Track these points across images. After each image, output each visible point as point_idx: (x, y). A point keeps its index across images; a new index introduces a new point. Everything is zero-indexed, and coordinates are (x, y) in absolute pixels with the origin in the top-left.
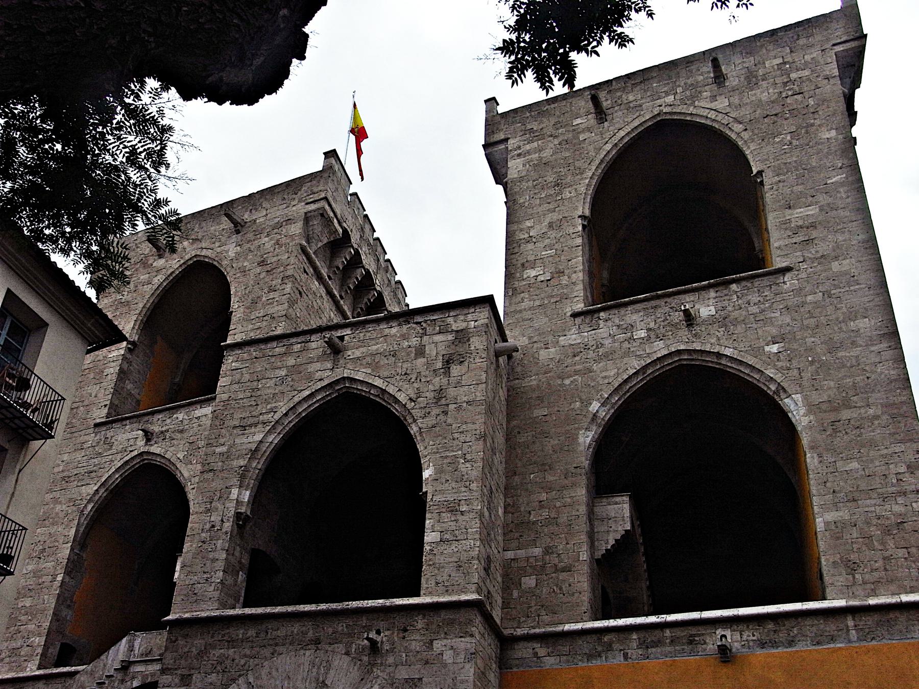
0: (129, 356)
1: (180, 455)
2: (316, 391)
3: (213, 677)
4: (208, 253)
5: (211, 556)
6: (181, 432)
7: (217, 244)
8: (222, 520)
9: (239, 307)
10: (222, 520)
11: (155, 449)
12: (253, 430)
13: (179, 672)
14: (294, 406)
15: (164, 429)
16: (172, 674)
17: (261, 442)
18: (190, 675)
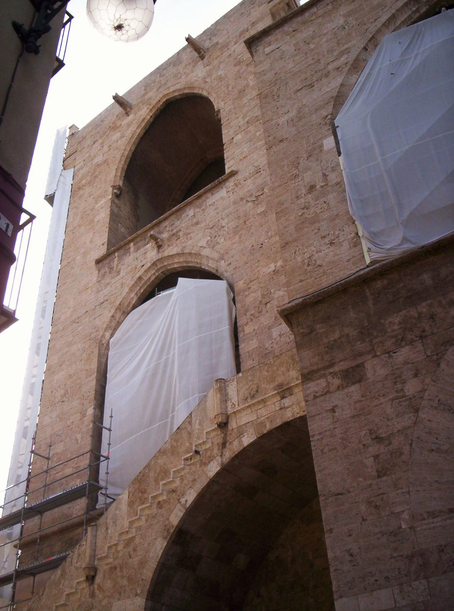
0: (116, 201)
1: (203, 243)
2: (398, 10)
3: (404, 353)
4: (178, 87)
5: (326, 215)
6: (197, 223)
7: (183, 77)
8: (324, 175)
9: (225, 104)
10: (324, 175)
11: (170, 250)
12: (324, 80)
13: (336, 368)
14: (373, 37)
15: (175, 231)
16: (324, 376)
17: (342, 85)
18: (358, 366)
